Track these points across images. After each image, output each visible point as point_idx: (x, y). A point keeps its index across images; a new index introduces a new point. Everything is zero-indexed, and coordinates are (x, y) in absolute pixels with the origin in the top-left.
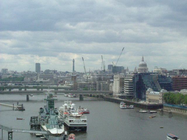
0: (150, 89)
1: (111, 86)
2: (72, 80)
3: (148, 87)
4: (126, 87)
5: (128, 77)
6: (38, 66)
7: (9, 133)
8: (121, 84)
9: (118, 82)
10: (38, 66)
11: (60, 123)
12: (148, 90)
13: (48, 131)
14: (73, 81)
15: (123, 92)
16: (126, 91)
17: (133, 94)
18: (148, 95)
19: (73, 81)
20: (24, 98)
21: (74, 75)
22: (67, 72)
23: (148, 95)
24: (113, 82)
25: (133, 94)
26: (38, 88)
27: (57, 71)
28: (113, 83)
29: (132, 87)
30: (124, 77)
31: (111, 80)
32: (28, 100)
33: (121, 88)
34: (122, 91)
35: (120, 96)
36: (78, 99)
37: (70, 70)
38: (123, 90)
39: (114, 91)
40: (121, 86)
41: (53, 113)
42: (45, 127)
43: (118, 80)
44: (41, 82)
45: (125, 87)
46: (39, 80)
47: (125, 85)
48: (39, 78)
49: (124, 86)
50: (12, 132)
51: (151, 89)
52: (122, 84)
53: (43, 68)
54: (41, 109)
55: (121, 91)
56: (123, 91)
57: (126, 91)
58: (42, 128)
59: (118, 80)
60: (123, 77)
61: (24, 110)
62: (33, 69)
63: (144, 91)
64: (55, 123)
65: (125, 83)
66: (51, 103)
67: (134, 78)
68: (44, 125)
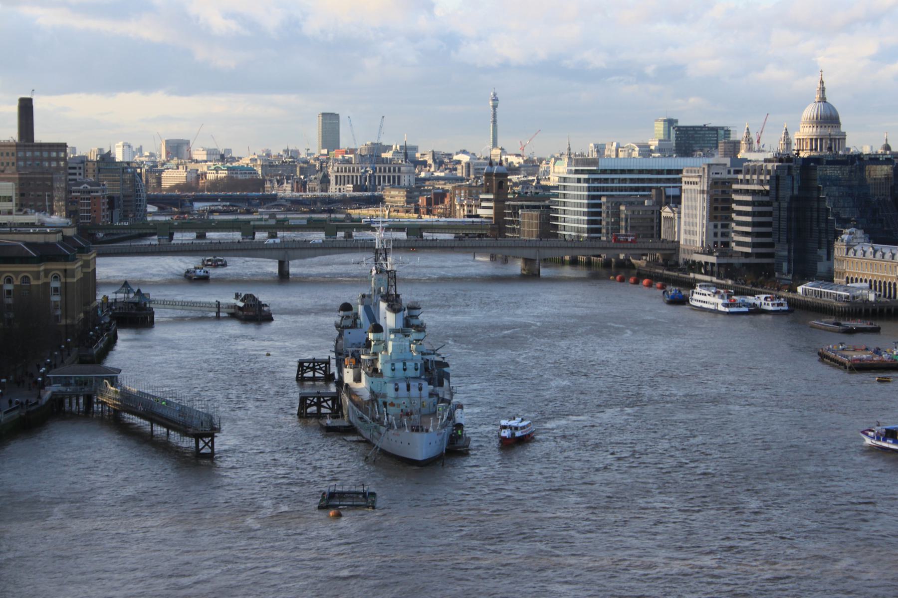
0: (853, 230)
1: (665, 218)
2: (488, 192)
3: (845, 223)
4: (739, 223)
5: (748, 177)
8: (716, 209)
9: (700, 197)
12: (845, 237)
14: (491, 196)
15: (726, 244)
16: (739, 244)
17: (771, 255)
19: (491, 196)
23: (841, 261)
25: (771, 255)
26: (330, 228)
28: (680, 203)
29: (769, 224)
30: (732, 176)
31: (671, 192)
33: (716, 226)
34: (720, 239)
35: (713, 264)
38: (723, 235)
39: (682, 242)
40: (716, 218)
43: (703, 192)
45: (733, 225)
47: (734, 215)
48: (333, 181)
49: (732, 220)
51: (859, 233)
52: (720, 206)
53: (355, 137)
55: (716, 243)
56: (725, 239)
57: (739, 244)
59: (703, 192)
60: (725, 175)
62: (309, 144)
63: (824, 241)
65: (734, 206)
67: (776, 180)
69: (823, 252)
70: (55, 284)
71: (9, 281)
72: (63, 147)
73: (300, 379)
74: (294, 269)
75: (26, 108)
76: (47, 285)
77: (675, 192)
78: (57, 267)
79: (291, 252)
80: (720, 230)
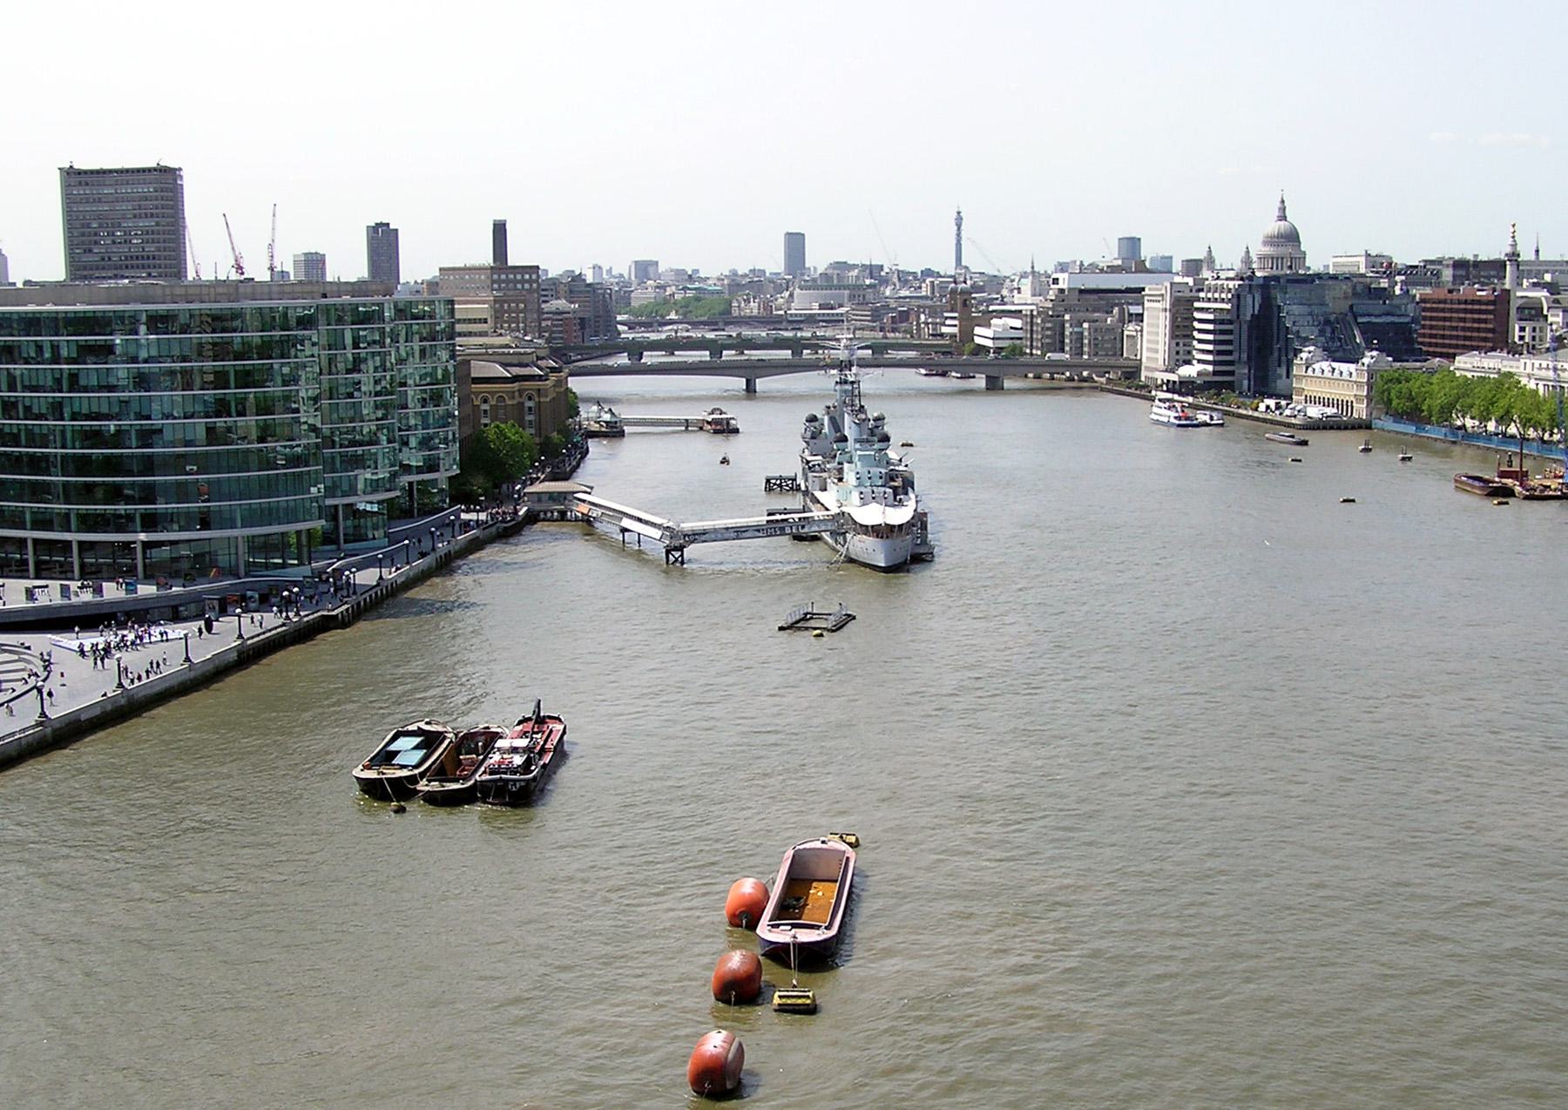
2: (952, 311)
3: (1305, 341)
4: (1200, 341)
9: (1162, 315)
10: (795, 244)
12: (1304, 355)
17: (1232, 373)
18: (1300, 378)
22: (928, 273)
23: (1300, 378)
24: (1140, 318)
25: (1232, 373)
30: (1194, 294)
31: (1135, 309)
37: (945, 265)
52: (1181, 328)
60: (1188, 294)
65: (1196, 324)
67: (1238, 297)
69: (1283, 371)
75: (500, 230)
77: (1138, 309)
79: (758, 372)
80: (1181, 349)
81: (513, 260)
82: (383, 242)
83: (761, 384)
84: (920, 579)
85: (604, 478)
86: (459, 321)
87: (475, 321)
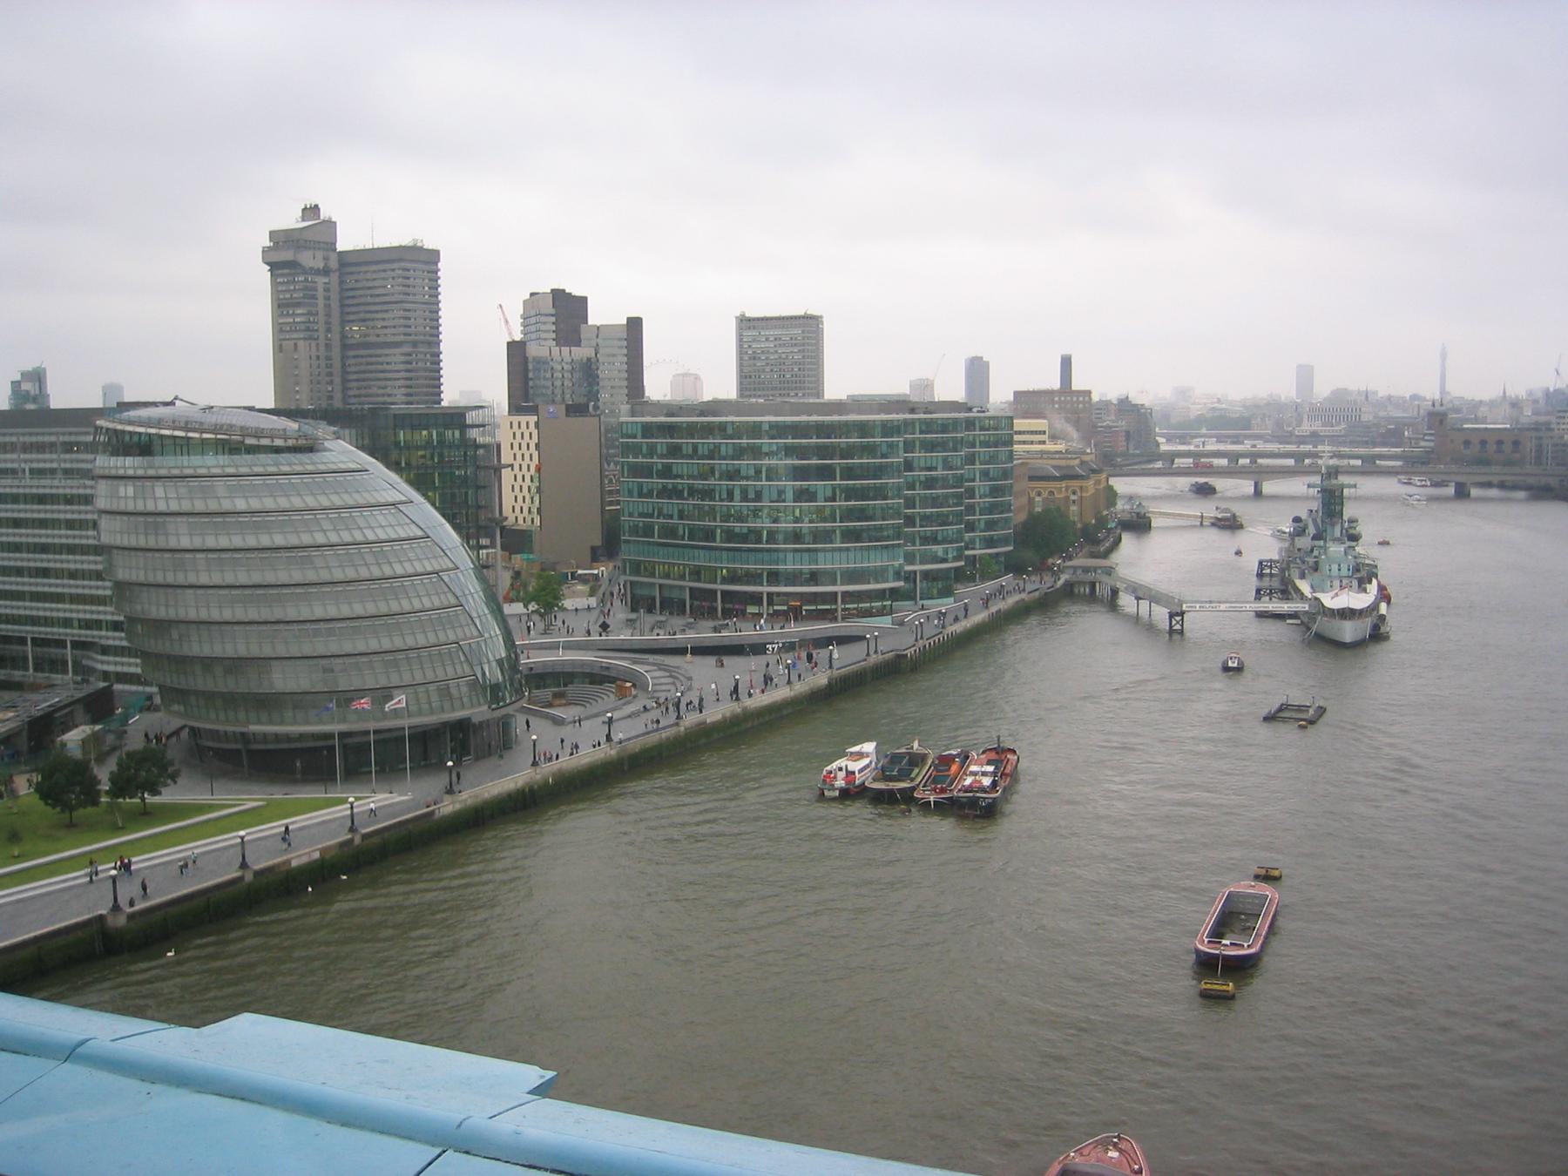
6: (1305, 375)
7: (1171, 616)
11: (1363, 573)
13: (1317, 599)
20: (1247, 487)
21: (1438, 408)
27: (1376, 393)
32: (1258, 493)
36: (1451, 491)
37: (1430, 392)
41: (1337, 533)
42: (1304, 586)
44: (1314, 434)
46: (1306, 428)
50: (1182, 614)
54: (1297, 520)
58: (1297, 590)
61: (1241, 527)
64: (1344, 572)
66: (1332, 502)
68: (1302, 576)
70: (1073, 497)
71: (1039, 494)
72: (1089, 392)
73: (1260, 575)
74: (1269, 487)
75: (1066, 363)
76: (1067, 498)
78: (1075, 484)
81: (1077, 385)
82: (977, 371)
83: (1269, 487)
84: (1379, 651)
85: (1138, 561)
86: (1020, 433)
87: (1036, 433)
